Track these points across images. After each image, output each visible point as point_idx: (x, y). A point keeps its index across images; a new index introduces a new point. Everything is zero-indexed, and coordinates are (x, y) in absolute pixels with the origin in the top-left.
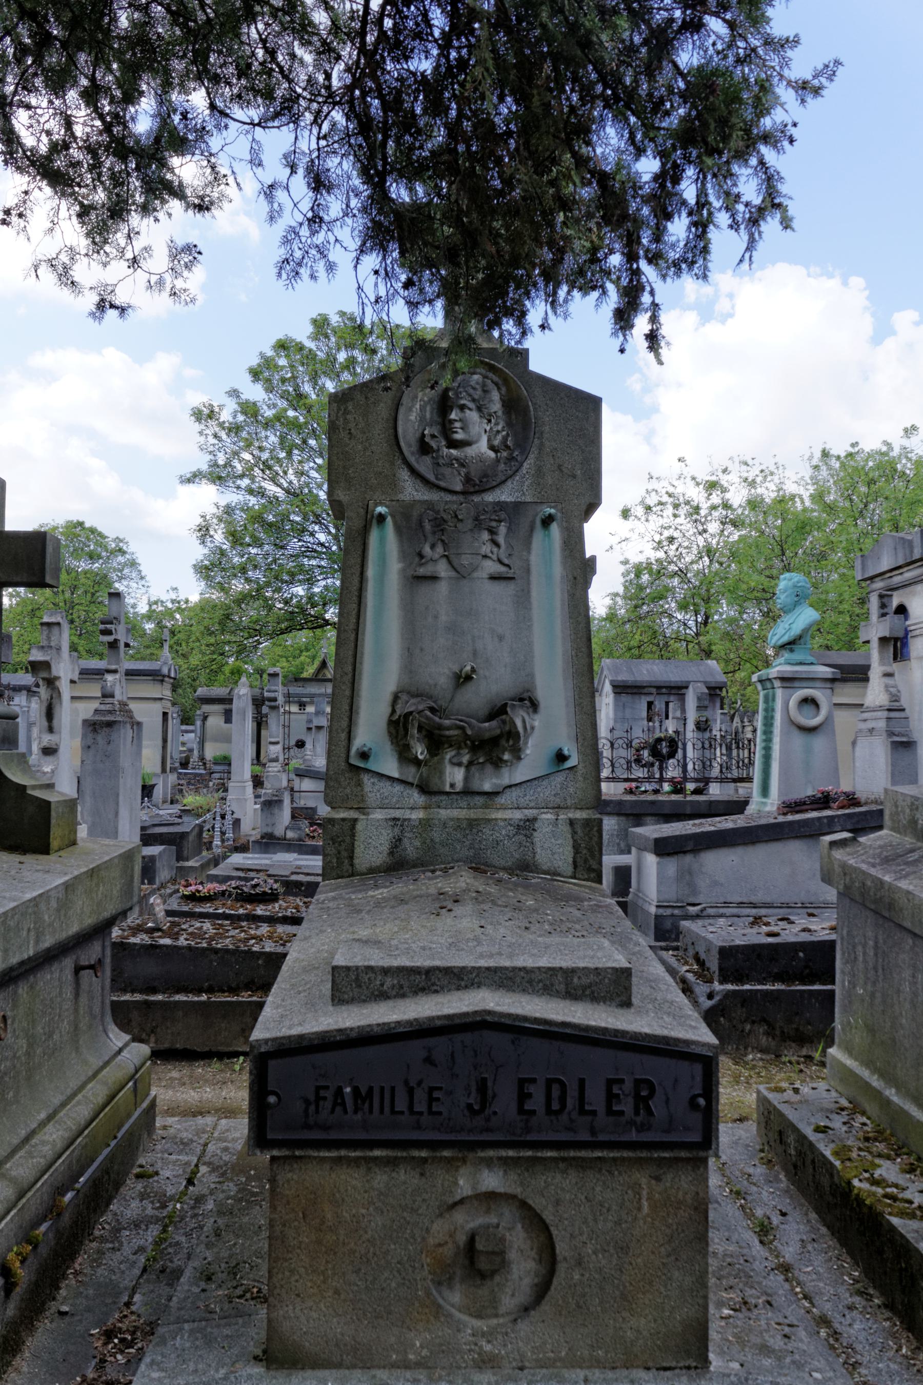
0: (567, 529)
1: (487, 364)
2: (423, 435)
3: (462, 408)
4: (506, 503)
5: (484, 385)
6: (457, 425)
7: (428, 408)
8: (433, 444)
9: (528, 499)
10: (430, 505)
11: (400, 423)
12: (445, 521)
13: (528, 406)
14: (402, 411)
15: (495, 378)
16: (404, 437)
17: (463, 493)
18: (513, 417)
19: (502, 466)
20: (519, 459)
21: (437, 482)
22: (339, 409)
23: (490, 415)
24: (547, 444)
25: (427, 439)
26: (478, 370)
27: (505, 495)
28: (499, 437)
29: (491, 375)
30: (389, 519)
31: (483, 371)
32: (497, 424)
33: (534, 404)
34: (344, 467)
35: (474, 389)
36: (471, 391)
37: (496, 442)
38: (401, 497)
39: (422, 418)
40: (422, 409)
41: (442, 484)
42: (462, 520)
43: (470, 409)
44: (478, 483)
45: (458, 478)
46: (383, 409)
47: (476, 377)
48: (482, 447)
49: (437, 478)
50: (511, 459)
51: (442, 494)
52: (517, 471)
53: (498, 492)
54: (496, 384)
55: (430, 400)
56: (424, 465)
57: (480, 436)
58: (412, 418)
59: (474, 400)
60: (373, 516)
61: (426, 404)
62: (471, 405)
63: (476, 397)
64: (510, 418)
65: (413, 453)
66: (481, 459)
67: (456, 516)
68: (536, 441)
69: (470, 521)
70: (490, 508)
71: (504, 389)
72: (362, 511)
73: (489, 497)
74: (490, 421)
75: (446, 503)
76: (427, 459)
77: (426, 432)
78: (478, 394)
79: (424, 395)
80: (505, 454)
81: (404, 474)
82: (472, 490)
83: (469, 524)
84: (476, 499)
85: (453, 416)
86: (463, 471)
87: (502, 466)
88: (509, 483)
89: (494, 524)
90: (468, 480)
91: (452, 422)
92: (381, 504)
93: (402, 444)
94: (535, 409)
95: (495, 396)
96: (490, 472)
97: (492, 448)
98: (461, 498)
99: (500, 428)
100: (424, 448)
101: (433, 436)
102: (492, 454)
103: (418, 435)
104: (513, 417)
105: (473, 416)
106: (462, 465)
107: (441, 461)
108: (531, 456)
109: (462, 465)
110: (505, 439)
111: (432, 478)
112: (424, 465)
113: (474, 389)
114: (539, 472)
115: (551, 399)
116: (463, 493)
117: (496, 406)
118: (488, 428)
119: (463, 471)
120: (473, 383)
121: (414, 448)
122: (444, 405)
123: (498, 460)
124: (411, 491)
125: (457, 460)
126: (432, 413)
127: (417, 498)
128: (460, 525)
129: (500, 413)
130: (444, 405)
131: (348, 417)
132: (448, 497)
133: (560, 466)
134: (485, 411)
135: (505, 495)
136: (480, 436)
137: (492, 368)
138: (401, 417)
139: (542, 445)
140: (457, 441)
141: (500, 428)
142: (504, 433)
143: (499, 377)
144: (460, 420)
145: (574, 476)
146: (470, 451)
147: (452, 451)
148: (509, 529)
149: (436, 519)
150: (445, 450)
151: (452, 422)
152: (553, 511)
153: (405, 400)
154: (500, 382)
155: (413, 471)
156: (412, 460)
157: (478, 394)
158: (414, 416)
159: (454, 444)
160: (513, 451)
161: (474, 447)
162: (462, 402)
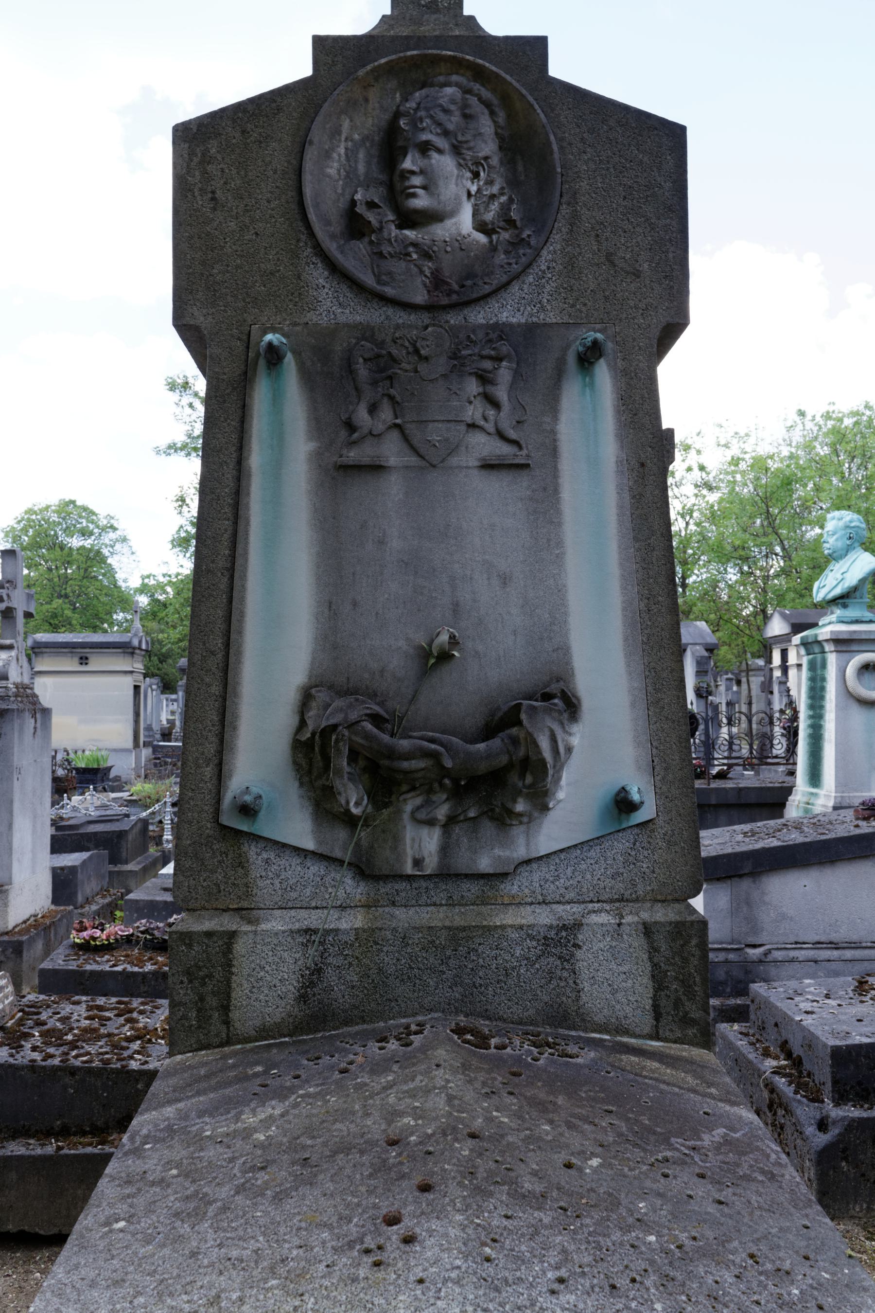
0: (625, 372)
2: (353, 203)
3: (425, 148)
4: (511, 325)
5: (465, 106)
6: (417, 181)
7: (361, 155)
8: (371, 217)
9: (552, 318)
10: (367, 333)
11: (307, 178)
12: (394, 360)
13: (549, 144)
15: (486, 94)
16: (317, 206)
17: (429, 308)
18: (520, 168)
20: (533, 242)
22: (192, 154)
23: (477, 163)
26: (455, 78)
27: (507, 311)
28: (495, 206)
29: (477, 87)
30: (289, 359)
32: (490, 182)
33: (560, 140)
35: (446, 111)
37: (489, 216)
38: (311, 317)
39: (350, 175)
40: (351, 155)
41: (389, 291)
42: (426, 359)
43: (440, 151)
44: (458, 287)
45: (419, 281)
47: (449, 90)
48: (464, 221)
49: (379, 282)
50: (518, 243)
51: (390, 311)
52: (529, 265)
53: (494, 304)
54: (487, 105)
56: (355, 258)
57: (459, 206)
59: (446, 133)
60: (258, 355)
63: (451, 127)
65: (333, 237)
66: (460, 243)
67: (417, 351)
68: (565, 210)
69: (443, 360)
70: (481, 335)
73: (479, 316)
74: (476, 175)
75: (397, 327)
76: (361, 247)
77: (358, 197)
78: (453, 122)
79: (353, 128)
80: (505, 235)
81: (318, 275)
82: (445, 301)
83: (441, 365)
84: (454, 319)
85: (407, 164)
86: (428, 267)
88: (515, 288)
89: (488, 365)
90: (437, 282)
92: (274, 330)
93: (312, 216)
94: (561, 148)
95: (486, 125)
97: (481, 226)
99: (495, 189)
100: (355, 225)
101: (371, 205)
102: (482, 238)
103: (343, 204)
104: (520, 168)
105: (445, 163)
106: (427, 255)
107: (386, 249)
108: (556, 237)
110: (505, 209)
111: (369, 280)
112: (355, 258)
113: (446, 111)
116: (429, 308)
117: (488, 148)
118: (474, 189)
119: (428, 267)
121: (337, 227)
122: (391, 145)
123: (493, 248)
124: (331, 307)
125: (415, 245)
126: (368, 163)
127: (342, 319)
128: (422, 368)
129: (495, 161)
130: (391, 145)
131: (209, 168)
132: (401, 317)
134: (468, 154)
135: (507, 311)
136: (459, 206)
137: (479, 74)
139: (575, 217)
140: (416, 211)
141: (495, 189)
142: (503, 199)
143: (494, 91)
144: (422, 172)
145: (637, 274)
146: (441, 231)
147: (407, 232)
148: (517, 374)
150: (394, 232)
152: (599, 336)
153: (316, 134)
154: (495, 101)
155: (334, 268)
156: (331, 247)
157: (453, 122)
158: (335, 172)
159: (410, 219)
160: (522, 230)
161: (449, 223)
162: (424, 137)
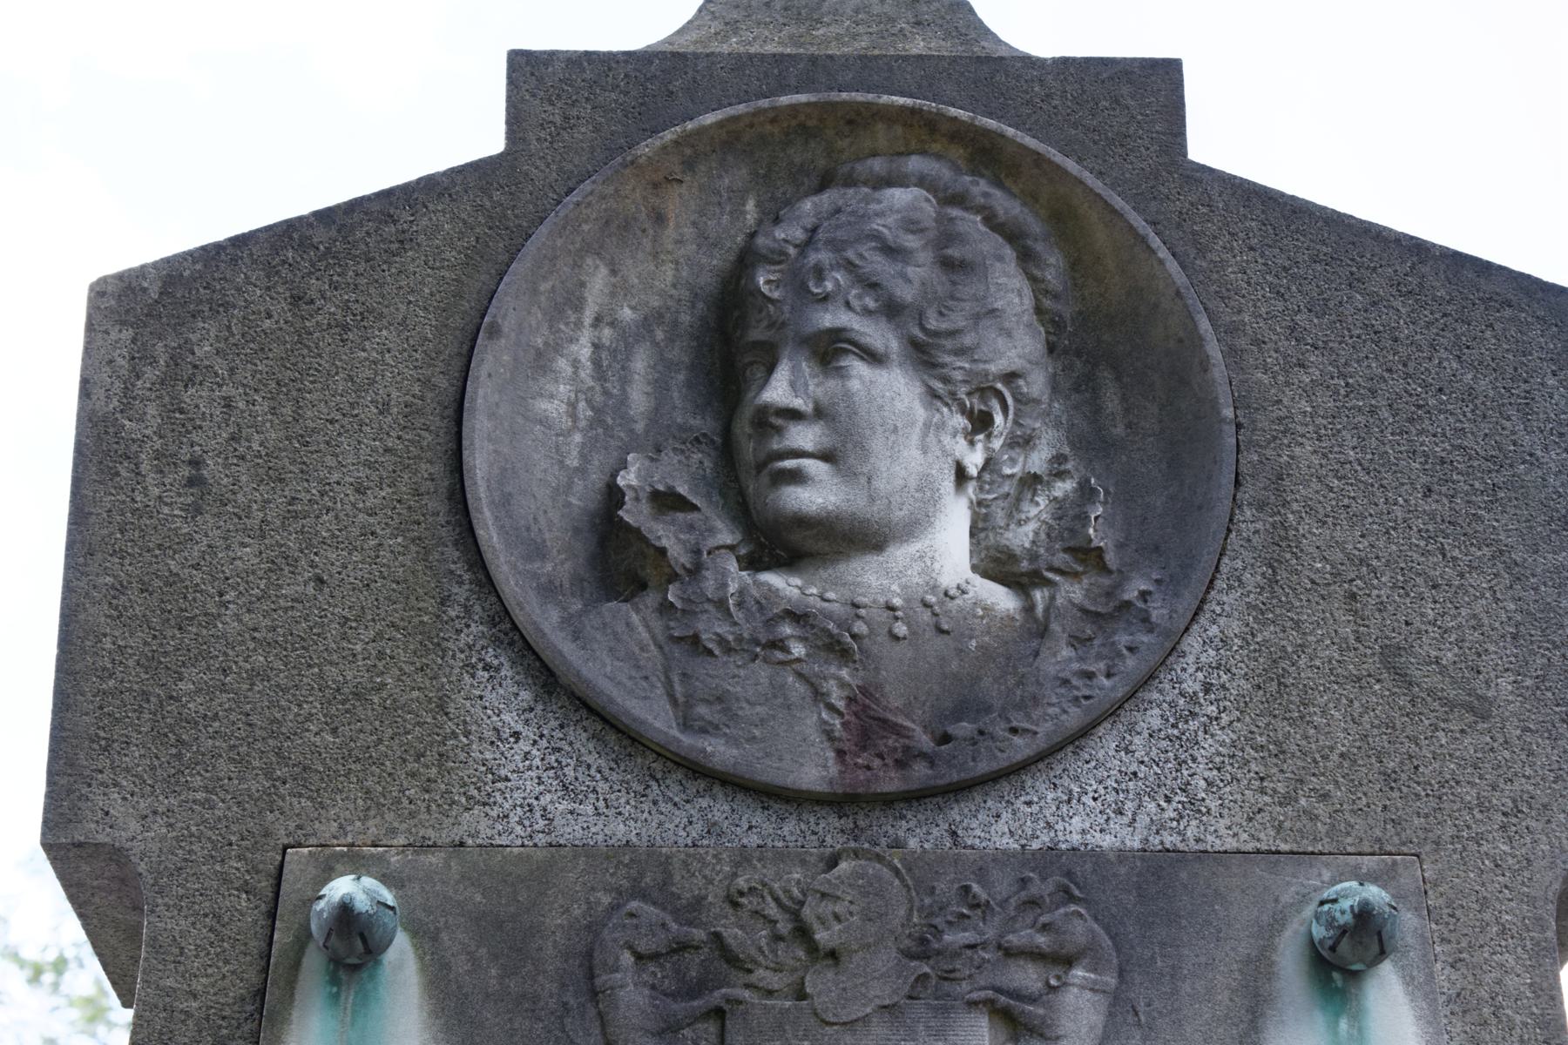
0: (1460, 1003)
1: (960, 134)
2: (614, 496)
3: (830, 350)
4: (1096, 855)
5: (947, 237)
6: (804, 436)
7: (640, 363)
8: (668, 536)
9: (1223, 835)
10: (645, 874)
11: (478, 426)
12: (731, 959)
13: (1198, 341)
14: (491, 362)
15: (1007, 206)
16: (504, 503)
17: (840, 802)
18: (1111, 402)
19: (1060, 656)
20: (1158, 612)
21: (687, 742)
22: (140, 357)
23: (985, 391)
24: (1311, 533)
25: (634, 514)
26: (915, 164)
27: (1087, 812)
28: (1038, 509)
29: (980, 188)
30: (401, 953)
31: (939, 170)
32: (1022, 442)
33: (1228, 331)
34: (150, 663)
35: (892, 251)
36: (878, 265)
37: (1021, 537)
38: (477, 825)
39: (606, 416)
40: (610, 363)
41: (718, 751)
42: (833, 955)
43: (873, 357)
44: (927, 744)
45: (810, 721)
46: (390, 365)
47: (899, 196)
48: (947, 549)
49: (686, 725)
50: (1109, 614)
51: (720, 809)
52: (1150, 678)
53: (1042, 793)
54: (1013, 235)
55: (648, 322)
56: (615, 654)
57: (929, 505)
58: (553, 408)
59: (892, 310)
60: (303, 938)
61: (629, 339)
62: (876, 334)
63: (906, 294)
64: (1095, 411)
65: (549, 590)
66: (937, 614)
67: (803, 932)
68: (1250, 522)
69: (886, 958)
70: (1003, 884)
71: (1053, 266)
72: (248, 911)
73: (998, 828)
74: (981, 423)
75: (743, 858)
76: (636, 621)
77: (628, 479)
78: (913, 279)
79: (619, 290)
80: (1073, 592)
81: (500, 702)
82: (891, 782)
83: (878, 976)
84: (919, 835)
85: (778, 391)
86: (839, 680)
87: (1060, 656)
88: (1106, 744)
89: (1028, 977)
90: (867, 725)
91: (771, 420)
92: (356, 864)
93: (489, 533)
94: (1232, 353)
95: (1010, 290)
96: (990, 688)
97: (996, 564)
98: (830, 830)
99: (1038, 461)
100: (616, 557)
101: (667, 502)
102: (1002, 599)
103: (584, 496)
104: (1111, 402)
105: (889, 392)
106: (836, 648)
107: (711, 628)
108: (1226, 598)
109: (836, 648)
110: (1069, 517)
111: (657, 718)
112: (615, 654)
113: (892, 251)
114: (1275, 681)
115: (1318, 307)
116: (840, 802)
117: (1016, 347)
118: (974, 460)
119: (839, 680)
120: (884, 226)
121: (561, 565)
122: (727, 343)
123: (1037, 629)
124: (536, 794)
125: (798, 616)
126: (660, 387)
127: (570, 831)
128: (820, 983)
129: (1036, 384)
130: (727, 343)
131: (188, 396)
132: (753, 827)
133: (1391, 656)
134: (959, 367)
135: (1087, 812)
136: (929, 505)
137: (986, 154)
138: (482, 393)
139: (1282, 540)
140: (802, 521)
141: (1038, 461)
142: (1063, 488)
143: (1030, 198)
144: (820, 413)
145: (1480, 709)
146: (877, 579)
147: (774, 579)
148: (1119, 1006)
149: (682, 947)
150: (737, 578)
151: (771, 420)
152: (1375, 893)
153: (509, 309)
154: (1035, 226)
155: (548, 680)
156: (544, 621)
157: (913, 279)
158: (559, 410)
159: (781, 543)
160: (1123, 577)
161: (900, 555)
162: (828, 319)
